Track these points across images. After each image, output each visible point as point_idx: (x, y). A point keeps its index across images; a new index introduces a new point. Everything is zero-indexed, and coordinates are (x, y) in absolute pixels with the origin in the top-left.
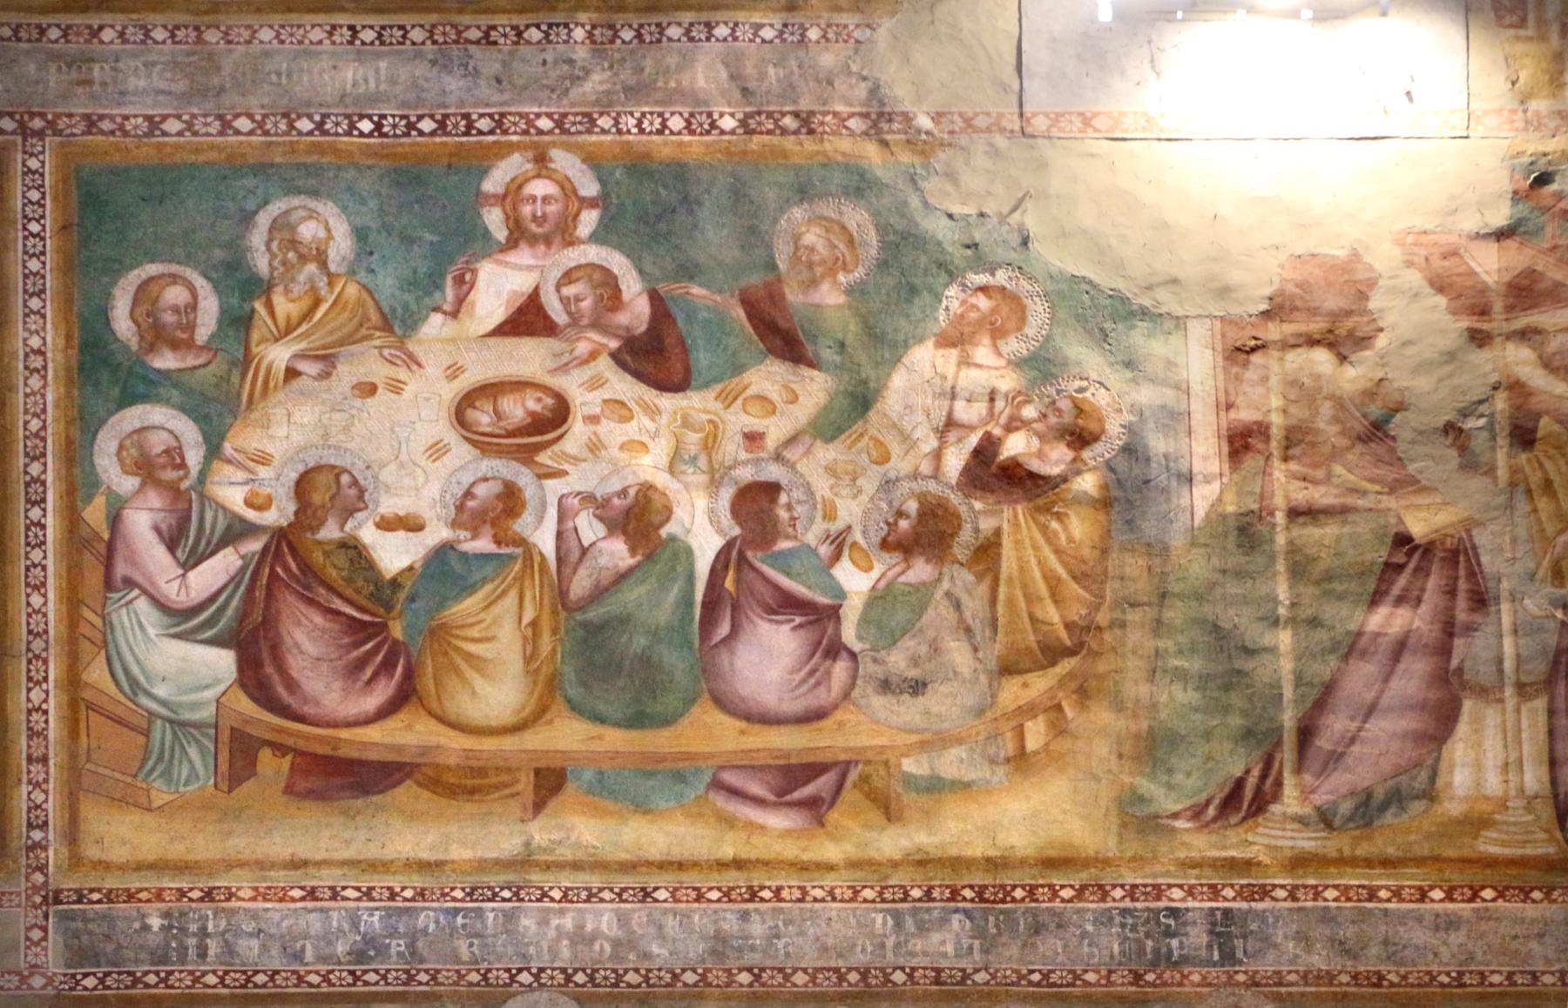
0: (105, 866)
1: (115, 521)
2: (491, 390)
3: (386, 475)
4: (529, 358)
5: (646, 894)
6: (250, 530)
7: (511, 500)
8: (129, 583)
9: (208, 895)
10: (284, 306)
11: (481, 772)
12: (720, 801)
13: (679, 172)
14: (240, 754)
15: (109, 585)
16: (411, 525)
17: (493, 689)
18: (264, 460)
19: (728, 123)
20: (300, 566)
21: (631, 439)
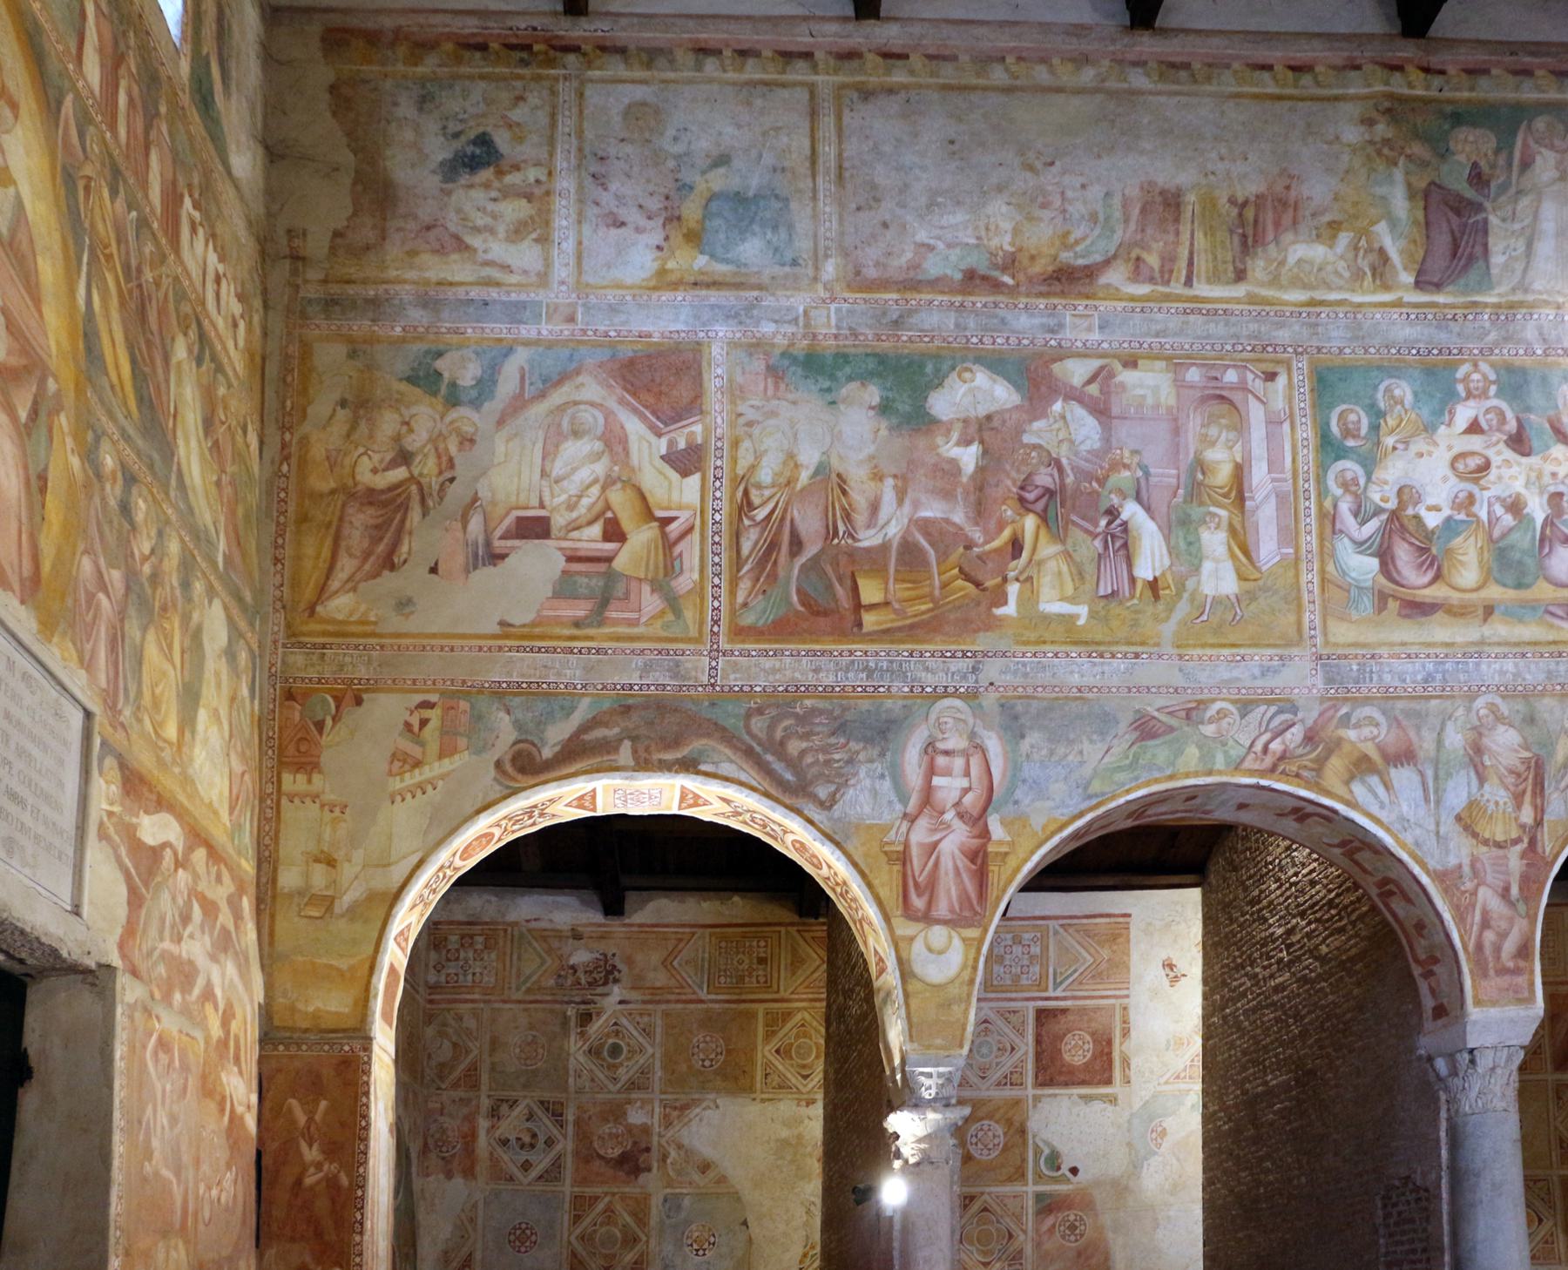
0: (1336, 645)
1: (1335, 506)
2: (1462, 456)
3: (1428, 489)
4: (1475, 443)
5: (1524, 655)
6: (1383, 510)
7: (1471, 499)
8: (1341, 532)
9: (1373, 657)
10: (1391, 422)
11: (1465, 607)
12: (1549, 618)
13: (1523, 371)
14: (1382, 599)
15: (1334, 533)
16: (1437, 509)
17: (1468, 574)
18: (1386, 483)
19: (1539, 352)
20: (1399, 523)
21: (1512, 475)
